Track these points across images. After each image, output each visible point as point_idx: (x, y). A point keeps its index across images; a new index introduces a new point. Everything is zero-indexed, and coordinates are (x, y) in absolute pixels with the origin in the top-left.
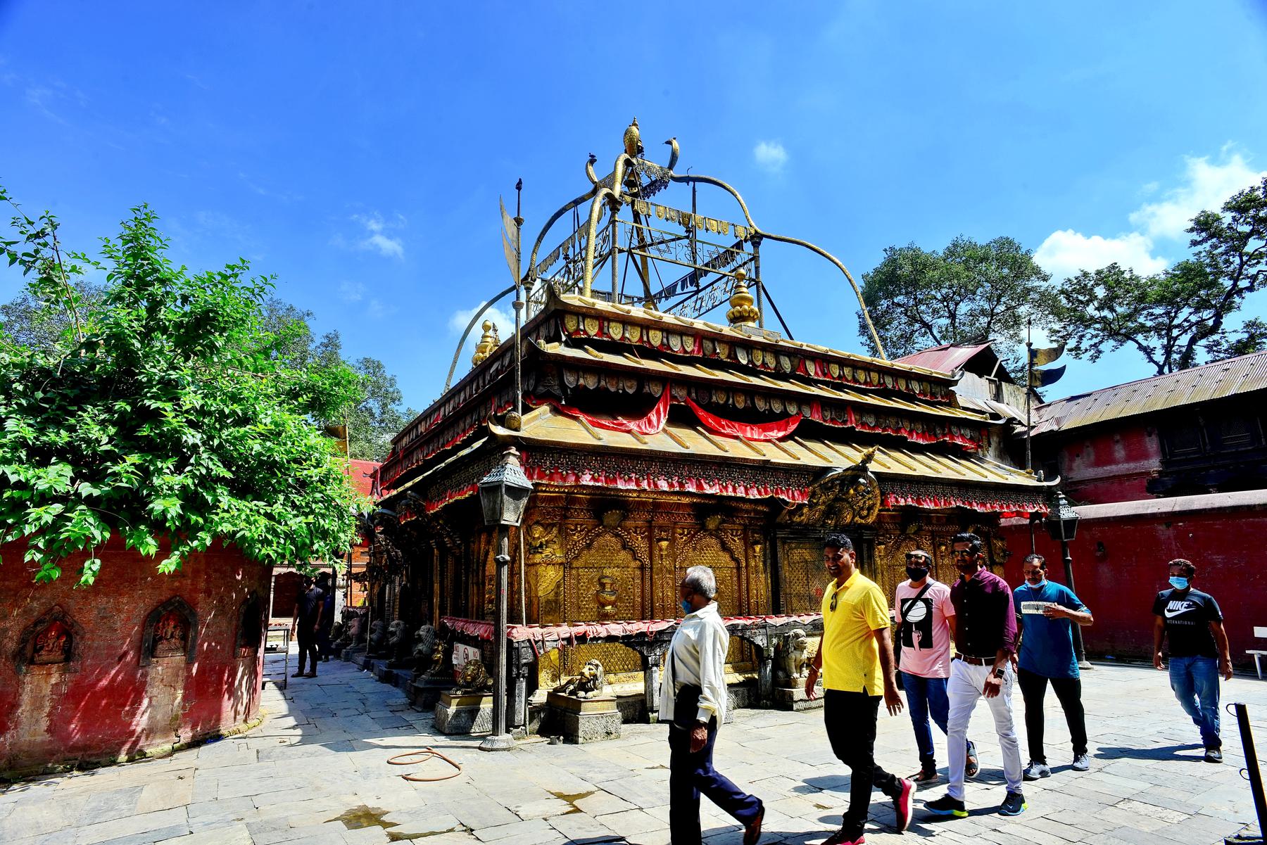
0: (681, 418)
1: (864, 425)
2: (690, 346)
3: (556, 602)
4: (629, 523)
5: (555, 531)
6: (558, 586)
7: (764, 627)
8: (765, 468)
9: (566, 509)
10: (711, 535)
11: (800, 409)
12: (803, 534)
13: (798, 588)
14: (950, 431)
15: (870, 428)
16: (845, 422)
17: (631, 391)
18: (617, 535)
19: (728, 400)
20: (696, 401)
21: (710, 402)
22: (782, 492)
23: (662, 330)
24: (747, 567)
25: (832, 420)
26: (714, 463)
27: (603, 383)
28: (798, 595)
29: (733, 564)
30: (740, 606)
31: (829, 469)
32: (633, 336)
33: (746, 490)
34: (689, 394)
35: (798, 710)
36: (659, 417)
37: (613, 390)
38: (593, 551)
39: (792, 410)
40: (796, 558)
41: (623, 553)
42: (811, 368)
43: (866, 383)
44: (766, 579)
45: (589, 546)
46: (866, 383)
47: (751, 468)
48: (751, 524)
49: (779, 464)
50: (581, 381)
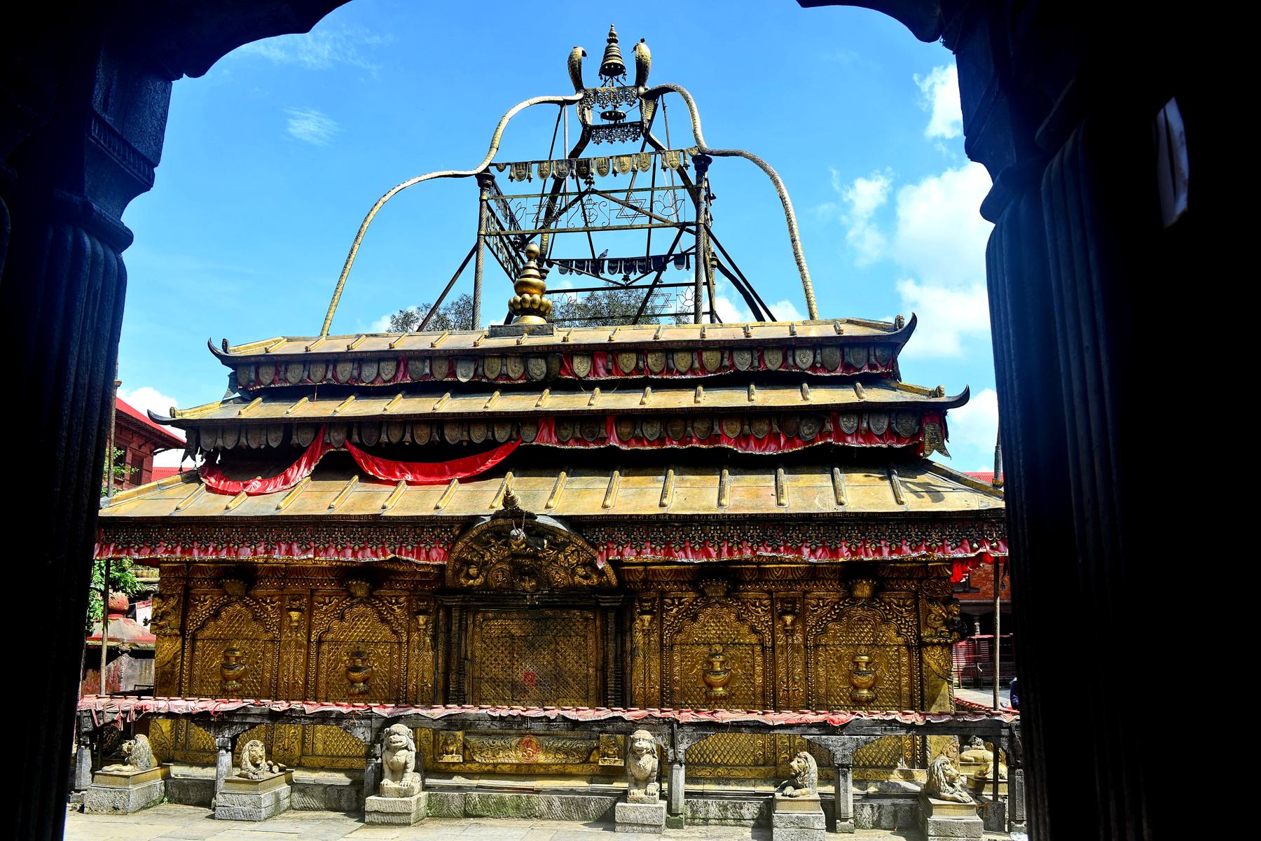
0: (334, 467)
1: (640, 440)
2: (388, 370)
3: (172, 673)
4: (260, 592)
5: (173, 602)
6: (175, 658)
7: (369, 718)
8: (376, 526)
9: (188, 579)
10: (361, 602)
11: (518, 433)
12: (497, 600)
13: (496, 671)
14: (837, 426)
15: (651, 443)
16: (604, 440)
17: (274, 445)
18: (247, 606)
19: (403, 436)
20: (361, 446)
21: (379, 444)
22: (407, 555)
23: (353, 361)
24: (408, 642)
25: (578, 441)
26: (339, 523)
27: (243, 440)
28: (494, 681)
29: (394, 638)
30: (398, 690)
31: (474, 519)
32: (318, 375)
33: (354, 554)
34: (349, 437)
35: (372, 824)
36: (301, 474)
37: (254, 446)
38: (220, 622)
39: (501, 435)
40: (495, 632)
41: (255, 625)
42: (581, 367)
43: (692, 370)
44: (436, 657)
45: (216, 615)
46: (692, 370)
47: (361, 525)
48: (415, 589)
49: (398, 518)
50: (220, 442)
